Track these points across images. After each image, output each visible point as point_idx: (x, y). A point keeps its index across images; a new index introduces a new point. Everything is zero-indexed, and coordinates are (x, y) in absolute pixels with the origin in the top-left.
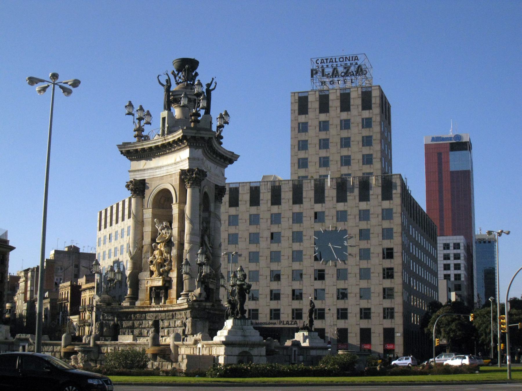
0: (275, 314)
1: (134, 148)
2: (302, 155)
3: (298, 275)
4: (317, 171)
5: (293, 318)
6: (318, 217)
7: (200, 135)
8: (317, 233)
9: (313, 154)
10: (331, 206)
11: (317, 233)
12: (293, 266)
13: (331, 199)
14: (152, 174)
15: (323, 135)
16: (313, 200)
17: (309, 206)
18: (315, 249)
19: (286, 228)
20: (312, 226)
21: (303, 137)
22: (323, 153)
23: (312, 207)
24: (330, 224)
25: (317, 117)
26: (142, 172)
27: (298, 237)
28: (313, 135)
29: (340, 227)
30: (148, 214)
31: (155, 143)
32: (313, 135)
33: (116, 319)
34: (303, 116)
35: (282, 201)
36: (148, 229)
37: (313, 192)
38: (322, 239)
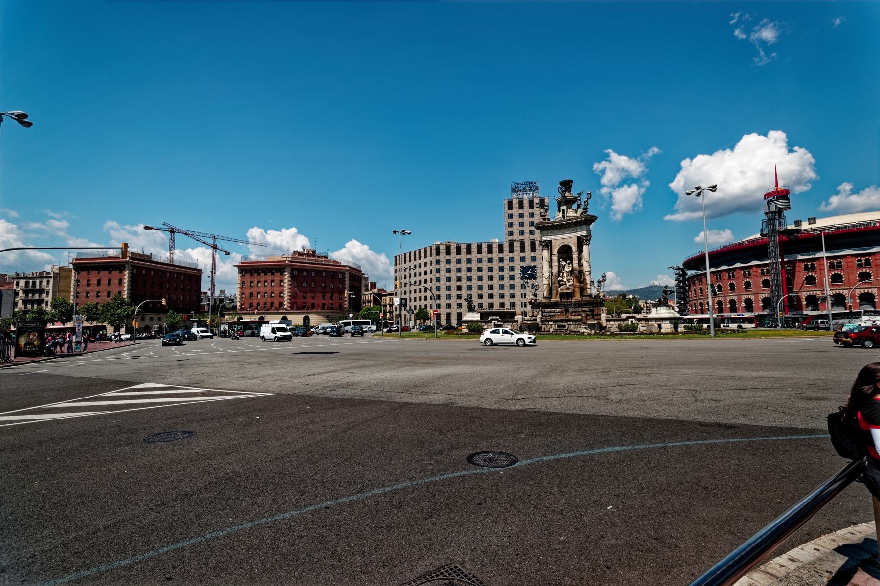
0: (491, 305)
2: (510, 229)
3: (448, 288)
6: (522, 259)
8: (522, 267)
9: (516, 229)
10: (528, 254)
11: (522, 267)
15: (521, 220)
17: (517, 254)
19: (506, 264)
21: (511, 221)
22: (521, 229)
24: (528, 263)
27: (512, 269)
28: (516, 220)
29: (533, 264)
30: (555, 258)
32: (516, 220)
36: (555, 264)
38: (524, 269)
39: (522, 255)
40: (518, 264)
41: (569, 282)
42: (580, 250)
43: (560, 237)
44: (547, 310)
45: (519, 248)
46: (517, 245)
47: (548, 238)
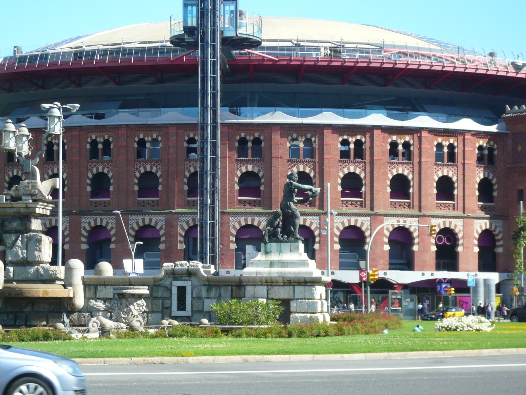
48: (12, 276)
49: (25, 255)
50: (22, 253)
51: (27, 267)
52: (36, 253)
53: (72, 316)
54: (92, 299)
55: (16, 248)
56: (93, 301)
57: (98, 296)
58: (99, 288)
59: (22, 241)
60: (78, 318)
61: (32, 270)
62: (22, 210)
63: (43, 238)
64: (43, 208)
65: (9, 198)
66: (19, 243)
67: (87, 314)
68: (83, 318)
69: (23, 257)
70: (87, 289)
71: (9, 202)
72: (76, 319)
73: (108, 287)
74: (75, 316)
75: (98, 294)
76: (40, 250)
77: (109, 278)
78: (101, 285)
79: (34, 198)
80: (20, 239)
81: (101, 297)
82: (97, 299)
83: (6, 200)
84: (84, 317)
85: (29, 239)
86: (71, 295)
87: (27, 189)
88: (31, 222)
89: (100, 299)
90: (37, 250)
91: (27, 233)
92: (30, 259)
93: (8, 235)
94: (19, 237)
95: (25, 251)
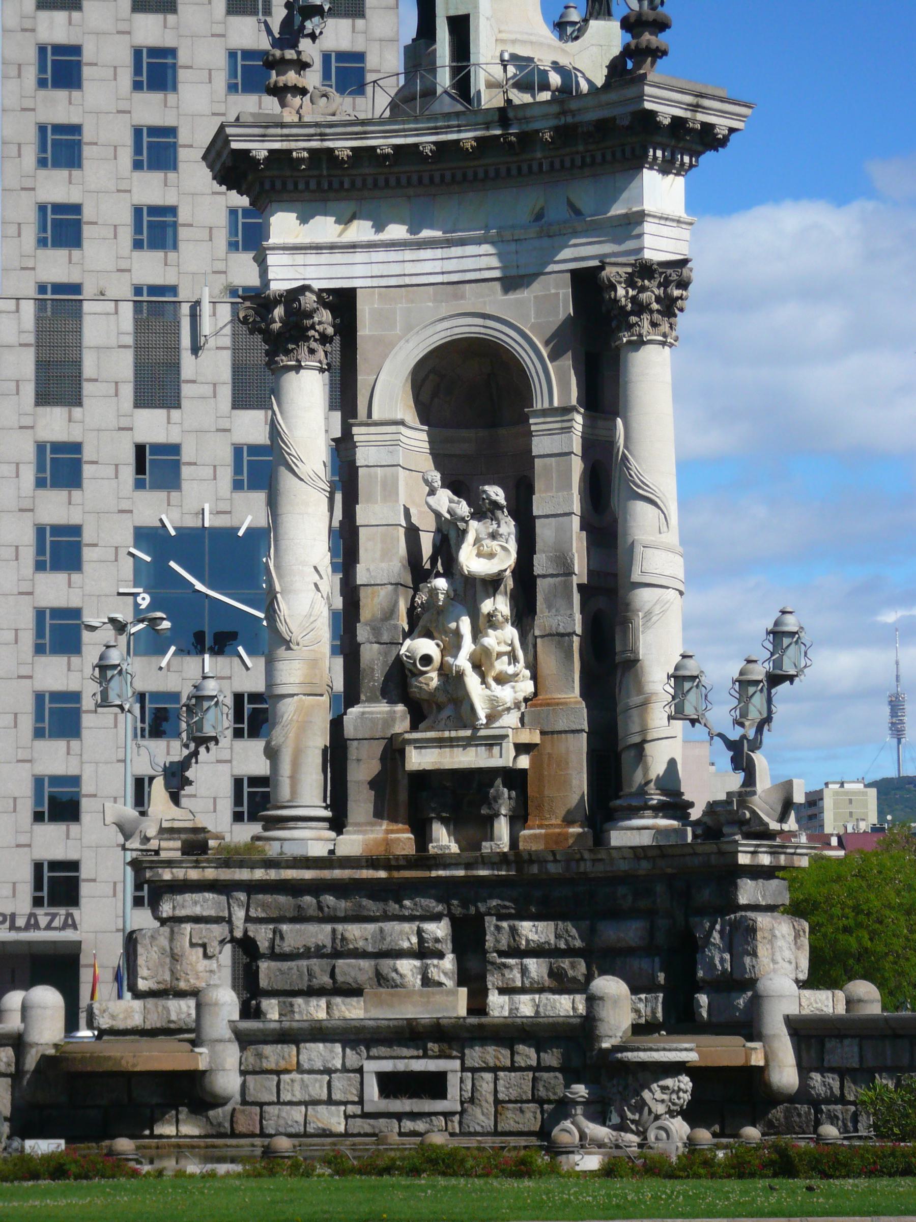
1: (315, 144)
4: (124, 265)
5: (37, 902)
7: (701, 117)
9: (108, 188)
10: (208, 421)
12: (38, 675)
13: (207, 390)
14: (396, 269)
16: (127, 391)
18: (137, 605)
20: (125, 505)
21: (59, 107)
23: (124, 423)
25: (123, 26)
26: (338, 257)
31: (436, 131)
33: (239, 915)
34: (60, 17)
35: (88, 388)
37: (128, 358)
39: (153, 426)
40: (111, 511)
41: (506, 687)
42: (603, 394)
43: (431, 264)
44: (295, 935)
45: (123, 366)
46: (107, 340)
47: (323, 274)
48: (705, 1015)
49: (728, 966)
50: (722, 961)
51: (734, 995)
52: (747, 960)
53: (774, 1111)
54: (817, 1070)
55: (710, 950)
56: (816, 1077)
57: (826, 1064)
58: (829, 1045)
59: (721, 932)
60: (786, 1118)
61: (741, 1001)
62: (714, 860)
63: (759, 925)
64: (771, 853)
65: (699, 831)
66: (716, 937)
67: (804, 1108)
68: (797, 1119)
69: (724, 971)
70: (803, 1046)
71: (699, 841)
72: (782, 1120)
73: (847, 1042)
74: (777, 1113)
75: (827, 1058)
76: (754, 954)
77: (872, 1021)
78: (831, 1036)
79: (744, 829)
80: (718, 927)
81: (834, 1065)
82: (822, 1070)
83: (695, 836)
84: (799, 1115)
85: (735, 926)
86: (757, 1060)
87: (729, 808)
88: (736, 886)
89: (832, 1070)
90: (749, 954)
91: (735, 913)
92: (737, 976)
93: (697, 919)
94: (716, 922)
95: (727, 956)
